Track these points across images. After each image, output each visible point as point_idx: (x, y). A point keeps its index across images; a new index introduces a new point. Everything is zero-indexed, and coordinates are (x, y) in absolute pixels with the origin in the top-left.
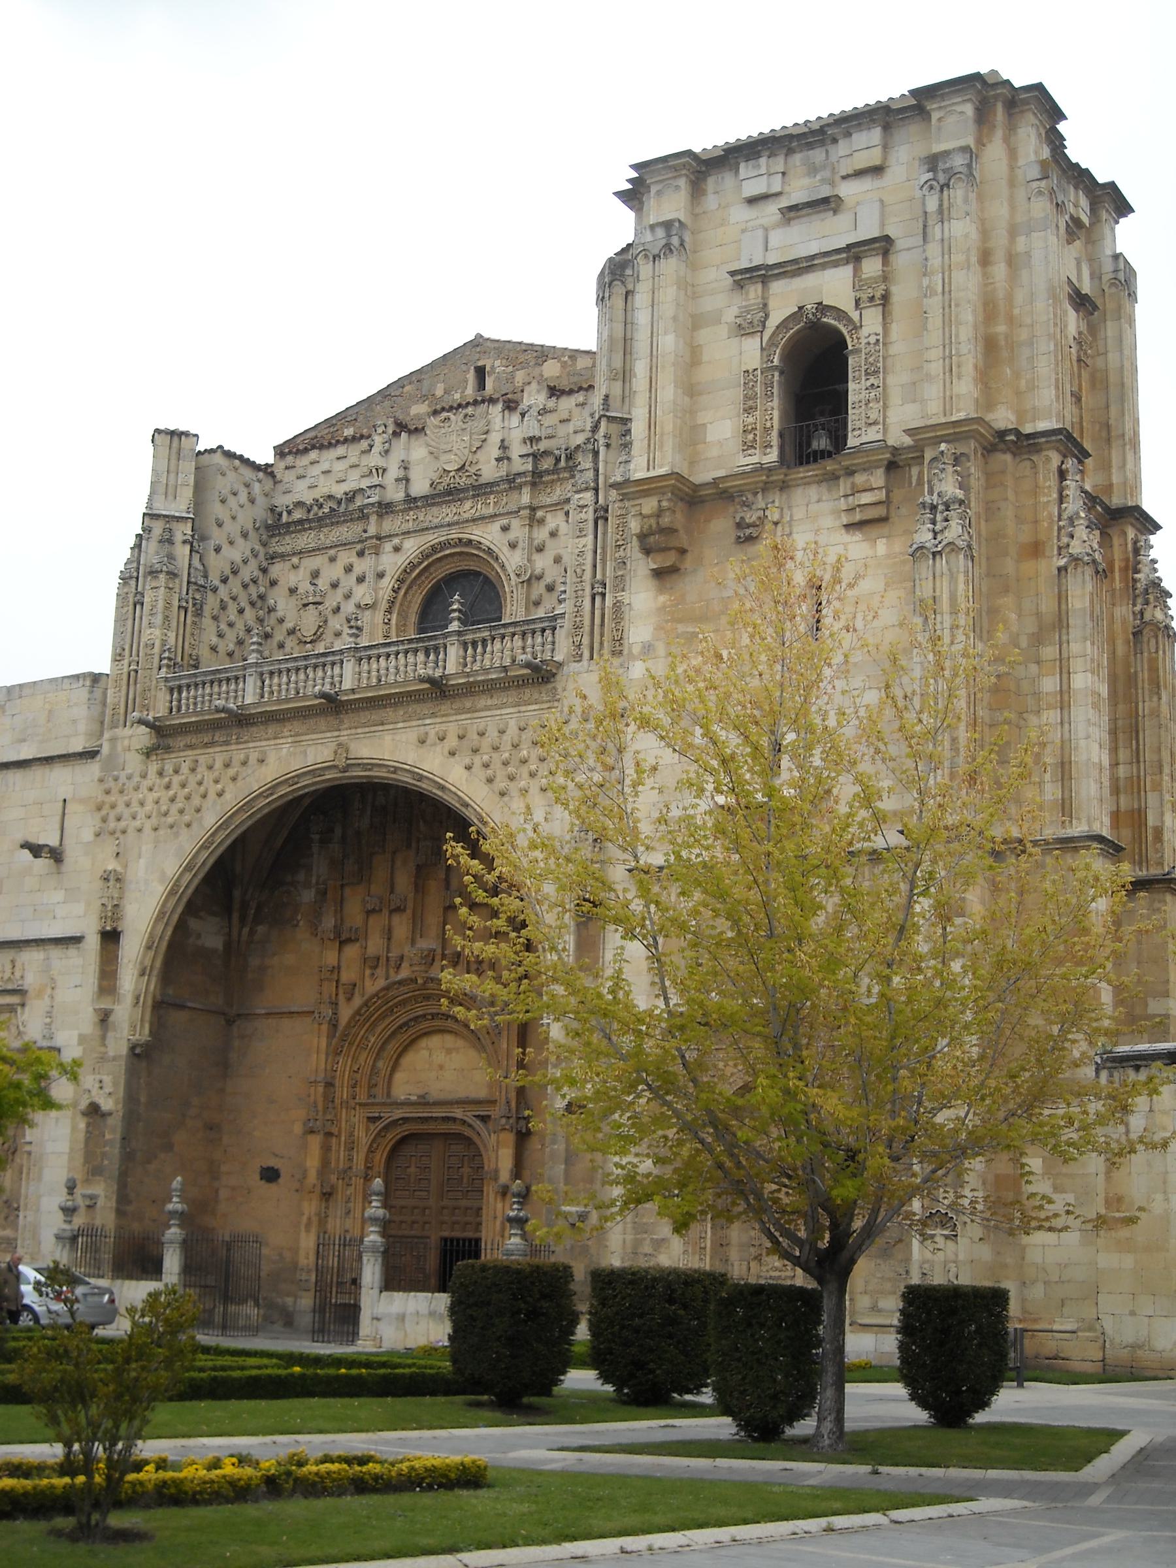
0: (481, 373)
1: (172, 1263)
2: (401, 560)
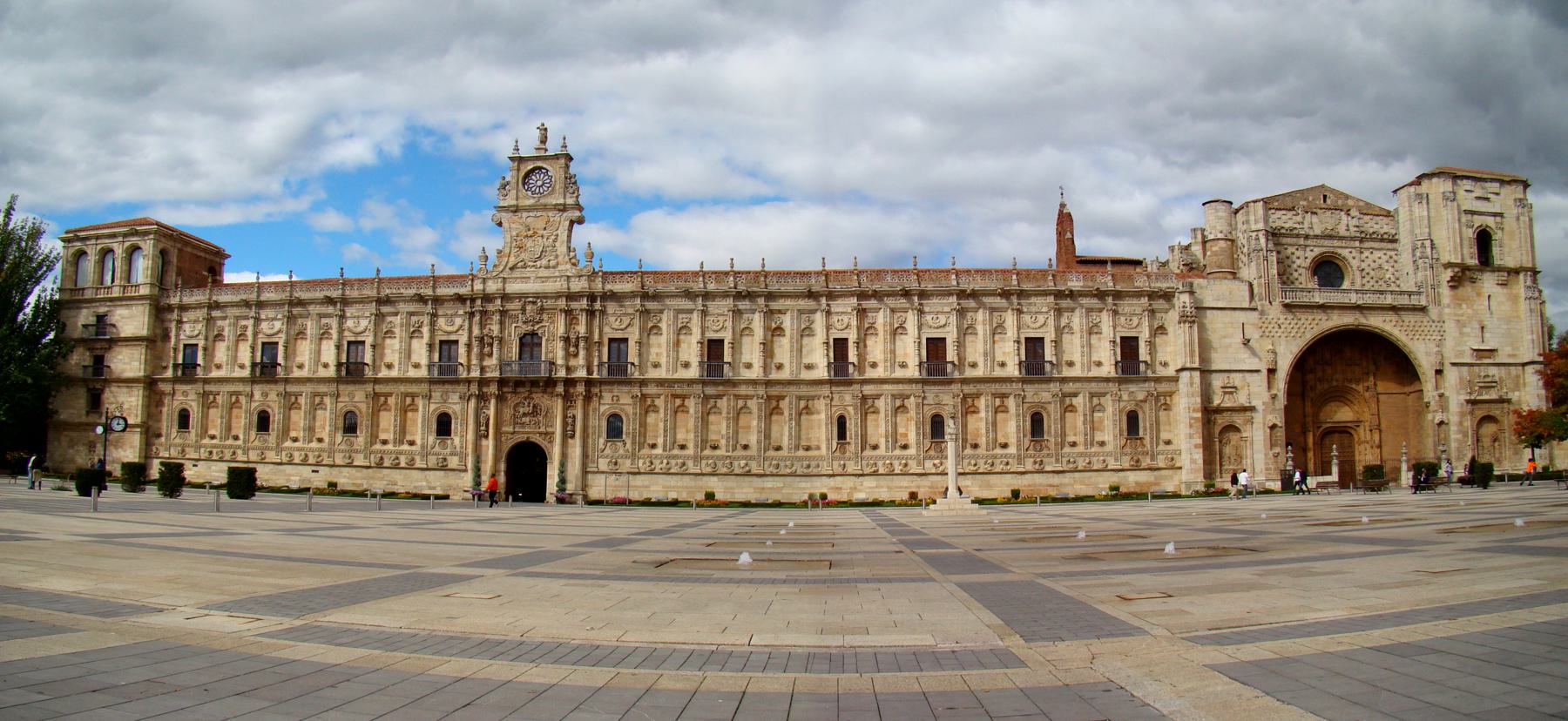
0: (1325, 197)
1: (1335, 470)
2: (1313, 255)
